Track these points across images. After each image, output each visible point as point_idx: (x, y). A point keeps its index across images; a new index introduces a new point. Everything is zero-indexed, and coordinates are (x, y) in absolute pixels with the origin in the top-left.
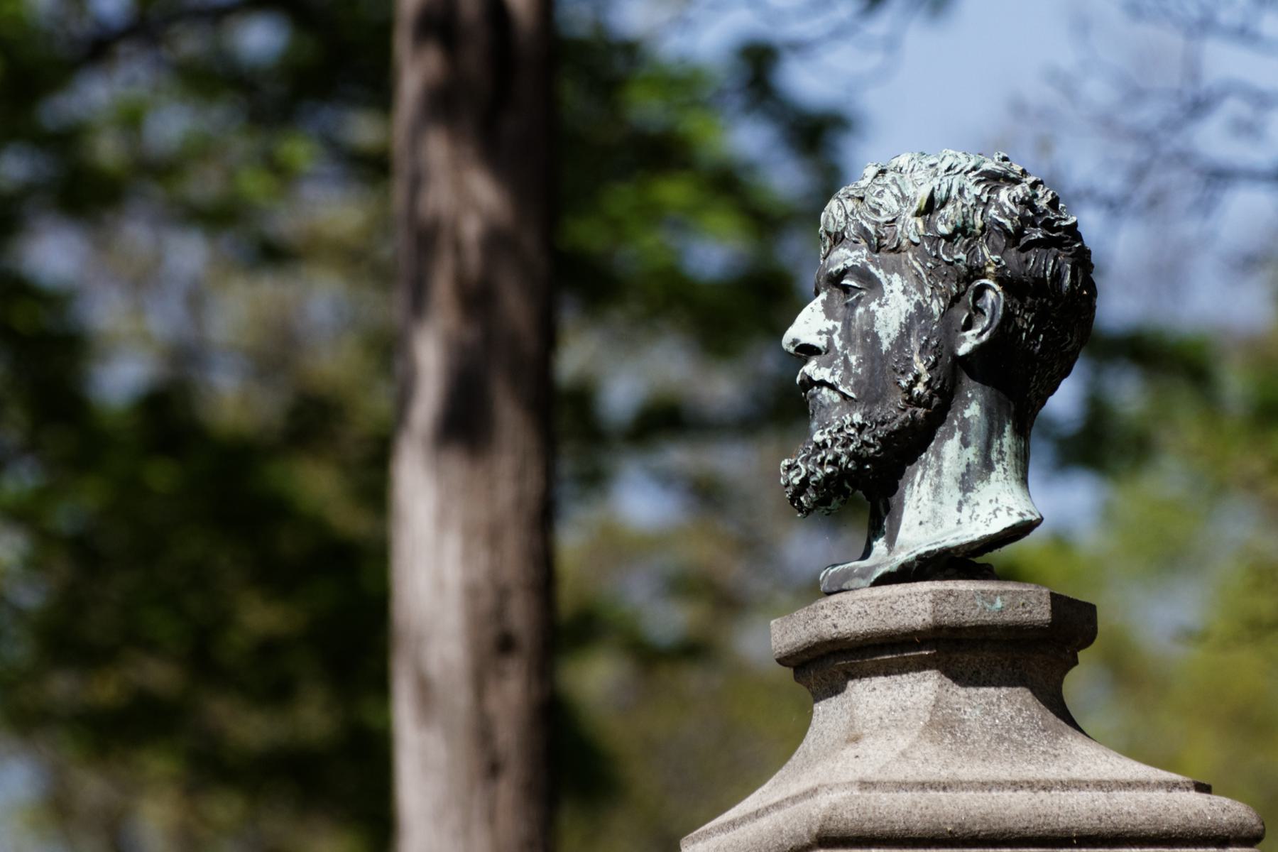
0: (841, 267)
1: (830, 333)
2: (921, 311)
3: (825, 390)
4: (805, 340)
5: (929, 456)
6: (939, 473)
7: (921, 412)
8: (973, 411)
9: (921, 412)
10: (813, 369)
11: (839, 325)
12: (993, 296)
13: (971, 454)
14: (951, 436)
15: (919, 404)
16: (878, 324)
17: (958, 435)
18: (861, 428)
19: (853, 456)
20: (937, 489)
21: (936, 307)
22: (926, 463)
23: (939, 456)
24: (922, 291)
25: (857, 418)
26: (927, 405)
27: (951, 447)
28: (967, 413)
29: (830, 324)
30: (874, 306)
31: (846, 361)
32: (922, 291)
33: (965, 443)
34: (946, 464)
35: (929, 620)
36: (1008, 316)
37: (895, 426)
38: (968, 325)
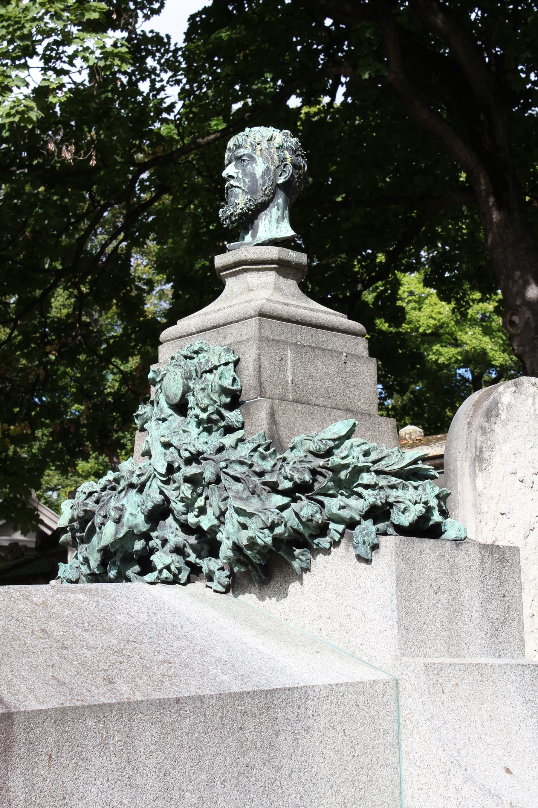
0: (242, 154)
1: (237, 173)
2: (268, 169)
3: (237, 189)
4: (230, 174)
5: (267, 212)
6: (271, 217)
7: (267, 198)
8: (280, 201)
9: (267, 198)
10: (232, 182)
11: (241, 171)
12: (290, 168)
13: (280, 213)
14: (274, 207)
15: (267, 196)
16: (255, 171)
17: (276, 207)
18: (250, 200)
19: (248, 208)
20: (270, 222)
21: (273, 168)
22: (266, 214)
23: (271, 212)
24: (269, 163)
25: (249, 197)
26: (269, 196)
27: (274, 210)
28: (279, 201)
29: (237, 171)
30: (254, 165)
31: (244, 181)
32: (269, 163)
33: (278, 210)
34: (273, 215)
35: (277, 256)
36: (292, 175)
37: (260, 201)
38: (281, 176)
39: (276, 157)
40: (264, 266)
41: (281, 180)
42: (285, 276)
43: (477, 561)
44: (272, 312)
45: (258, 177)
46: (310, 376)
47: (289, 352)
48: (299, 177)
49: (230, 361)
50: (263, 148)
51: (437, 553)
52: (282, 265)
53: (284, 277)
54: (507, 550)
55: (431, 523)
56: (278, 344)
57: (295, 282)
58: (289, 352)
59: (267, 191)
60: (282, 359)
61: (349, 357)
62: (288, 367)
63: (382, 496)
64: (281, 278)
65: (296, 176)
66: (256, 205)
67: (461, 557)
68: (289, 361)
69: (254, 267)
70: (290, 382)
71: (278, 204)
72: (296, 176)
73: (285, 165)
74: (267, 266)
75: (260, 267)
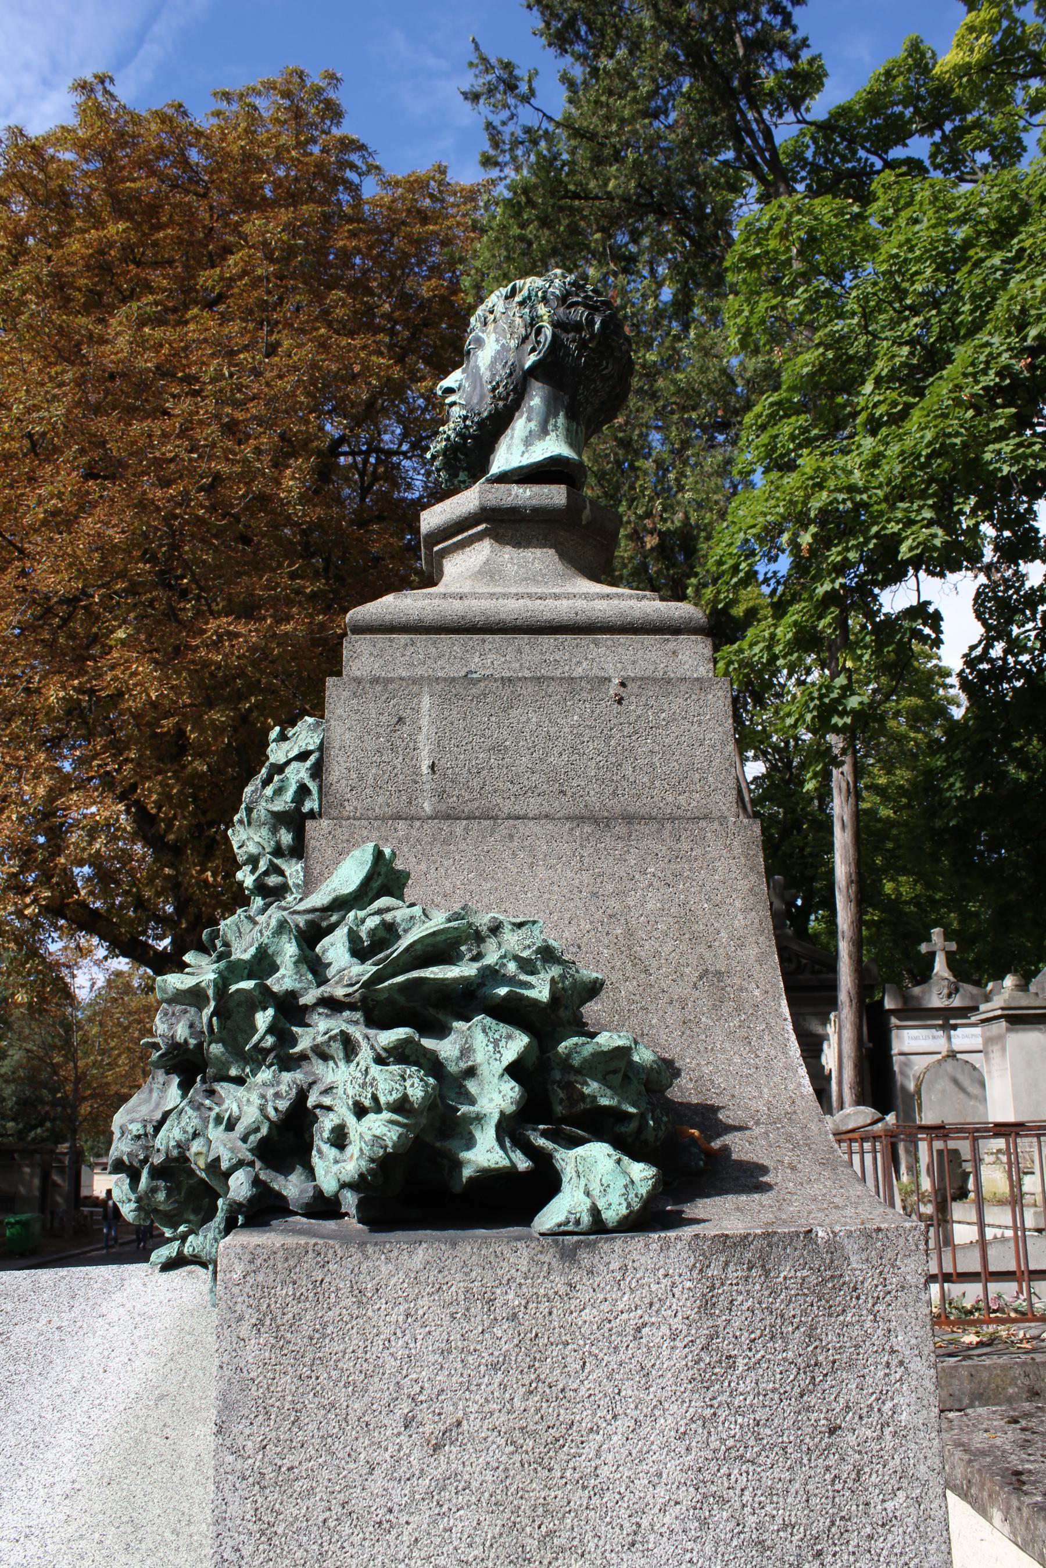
7: (501, 404)
13: (533, 425)
15: (500, 399)
17: (525, 416)
28: (532, 403)
33: (529, 420)
37: (485, 414)
39: (518, 321)
40: (465, 534)
41: (530, 360)
42: (519, 543)
43: (684, 1304)
44: (388, 617)
45: (482, 370)
46: (498, 749)
47: (426, 702)
48: (583, 345)
49: (311, 747)
50: (498, 315)
51: (457, 1287)
52: (502, 521)
53: (517, 545)
54: (851, 1247)
55: (467, 1172)
56: (390, 687)
57: (551, 552)
58: (426, 702)
59: (501, 389)
60: (400, 719)
61: (632, 687)
62: (421, 738)
63: (283, 1088)
64: (508, 549)
65: (573, 346)
66: (481, 424)
67: (584, 1294)
68: (425, 722)
69: (450, 542)
70: (425, 769)
71: (531, 409)
72: (573, 346)
73: (538, 332)
74: (470, 532)
75: (460, 537)
